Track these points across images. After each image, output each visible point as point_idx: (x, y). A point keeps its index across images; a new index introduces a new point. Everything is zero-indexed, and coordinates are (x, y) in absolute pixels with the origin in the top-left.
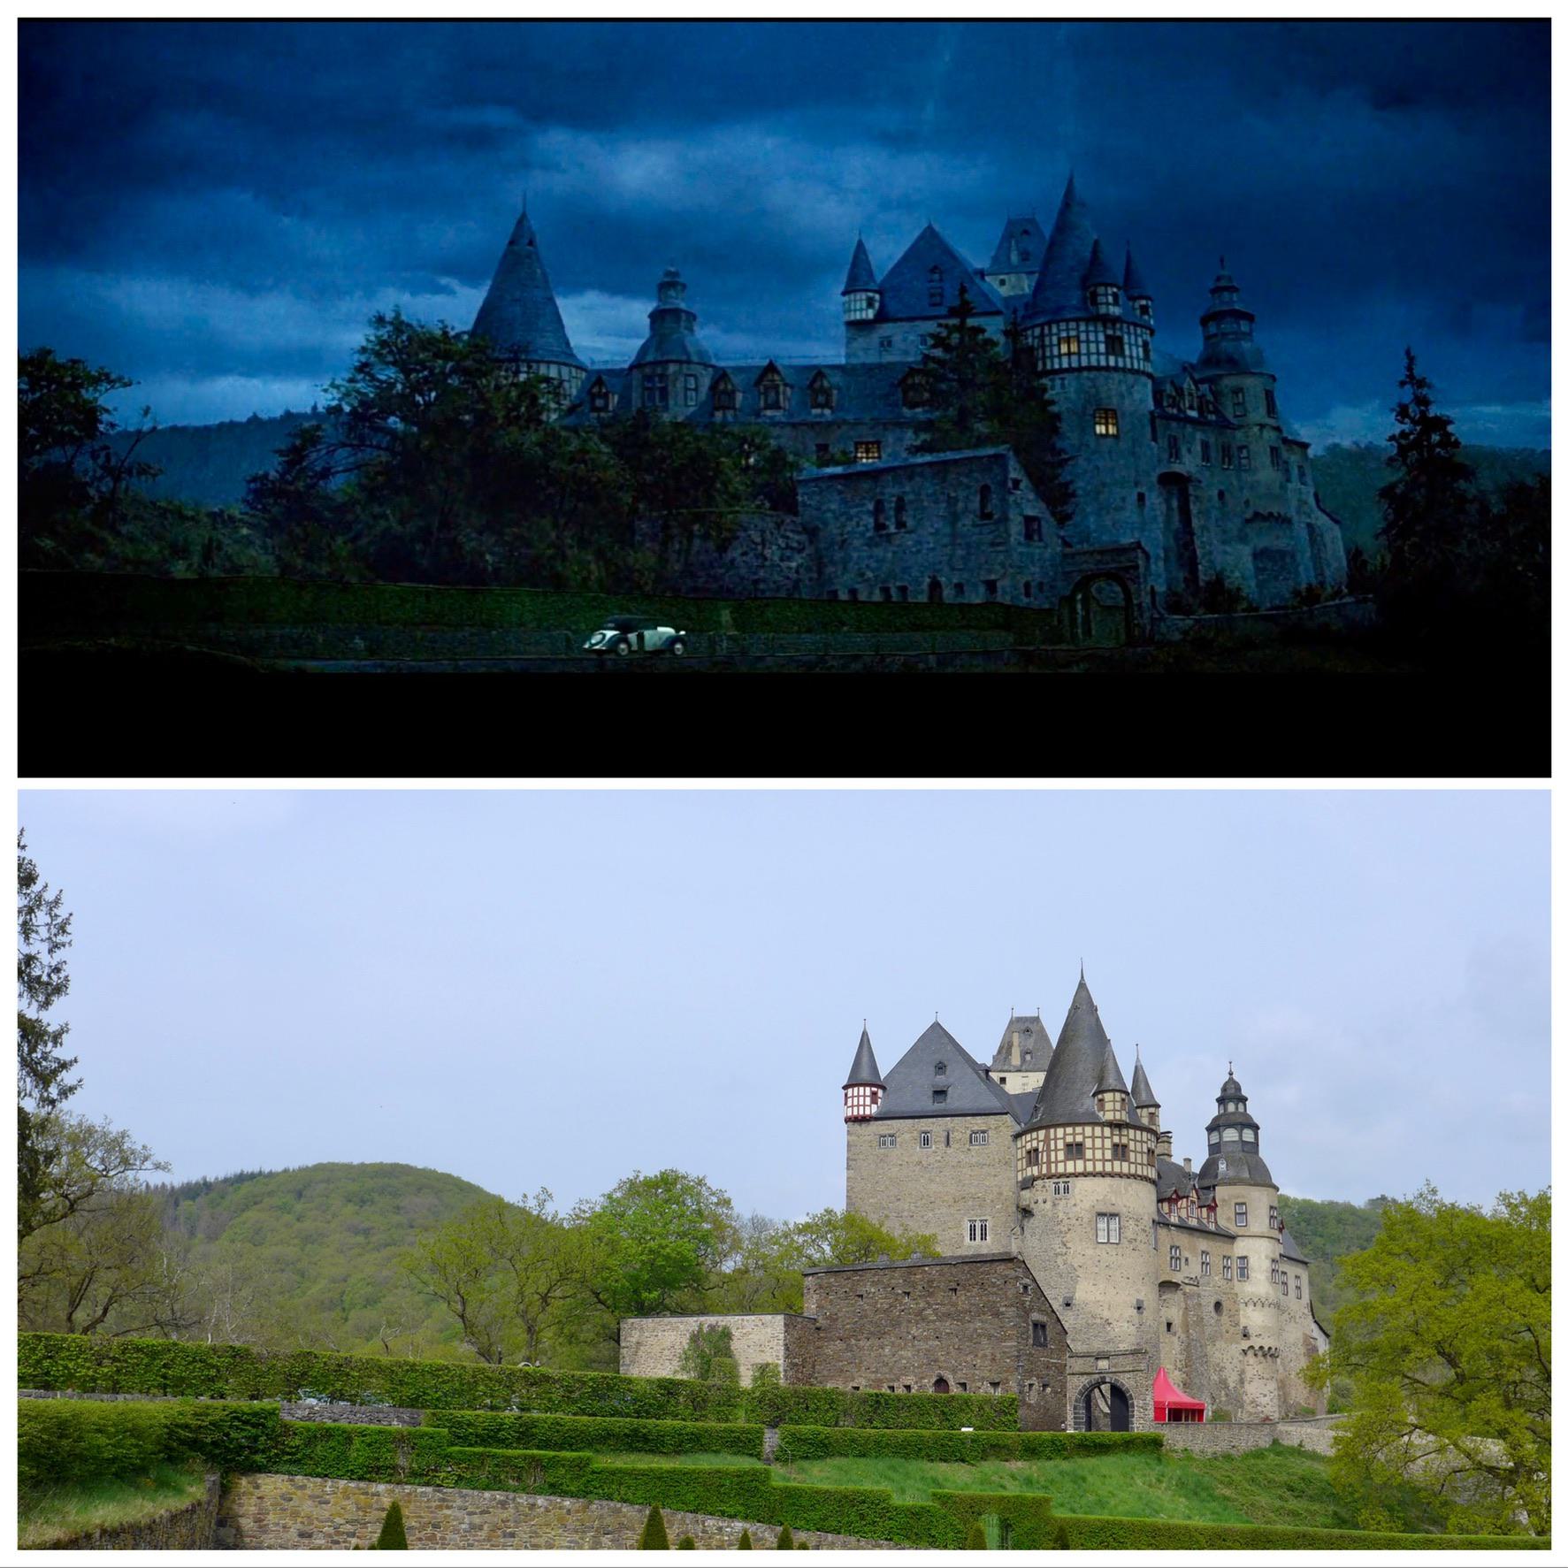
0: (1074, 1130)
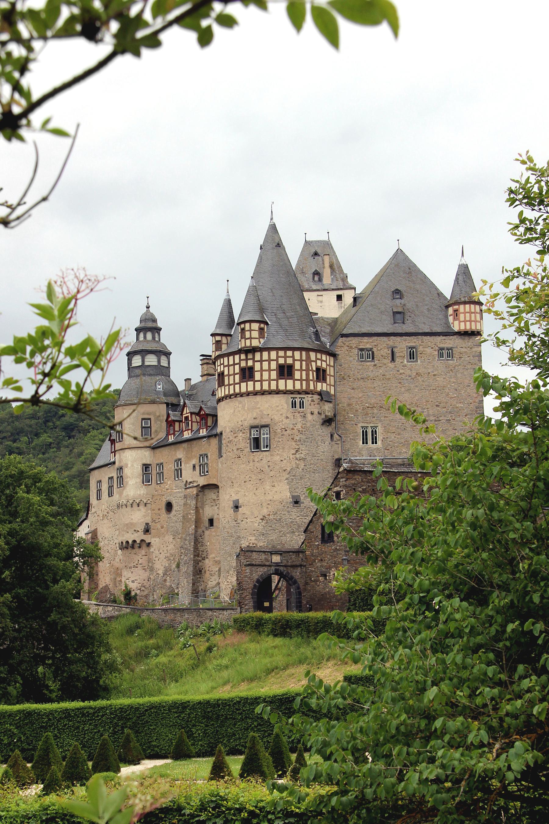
0: (285, 353)
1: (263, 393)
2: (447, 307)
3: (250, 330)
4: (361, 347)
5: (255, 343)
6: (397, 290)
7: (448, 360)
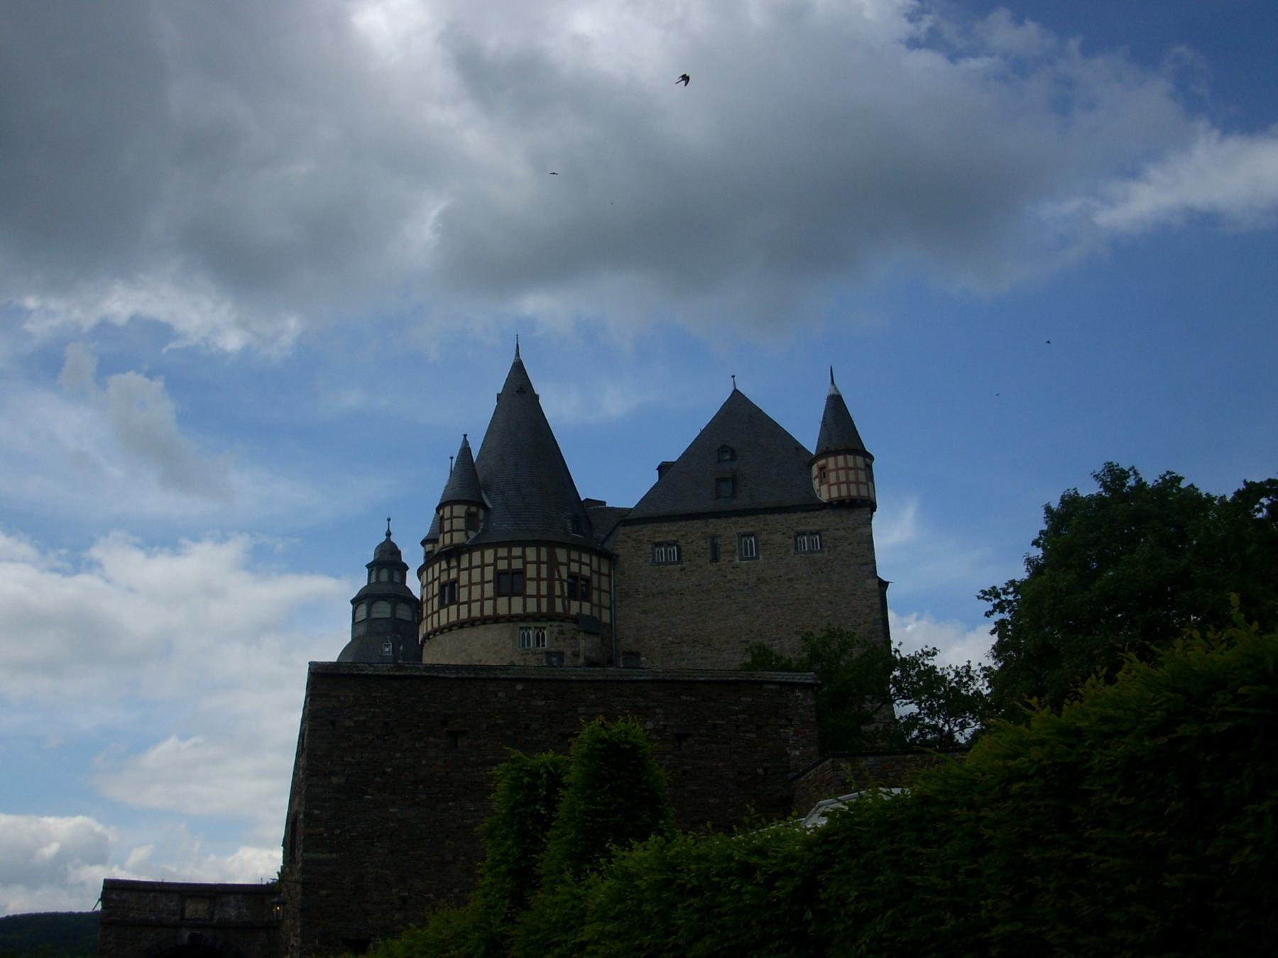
0: (510, 552)
1: (472, 623)
2: (810, 465)
3: (452, 518)
4: (657, 540)
5: (459, 538)
6: (724, 446)
7: (813, 552)
